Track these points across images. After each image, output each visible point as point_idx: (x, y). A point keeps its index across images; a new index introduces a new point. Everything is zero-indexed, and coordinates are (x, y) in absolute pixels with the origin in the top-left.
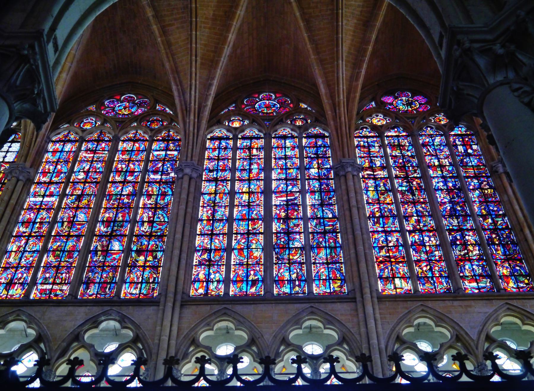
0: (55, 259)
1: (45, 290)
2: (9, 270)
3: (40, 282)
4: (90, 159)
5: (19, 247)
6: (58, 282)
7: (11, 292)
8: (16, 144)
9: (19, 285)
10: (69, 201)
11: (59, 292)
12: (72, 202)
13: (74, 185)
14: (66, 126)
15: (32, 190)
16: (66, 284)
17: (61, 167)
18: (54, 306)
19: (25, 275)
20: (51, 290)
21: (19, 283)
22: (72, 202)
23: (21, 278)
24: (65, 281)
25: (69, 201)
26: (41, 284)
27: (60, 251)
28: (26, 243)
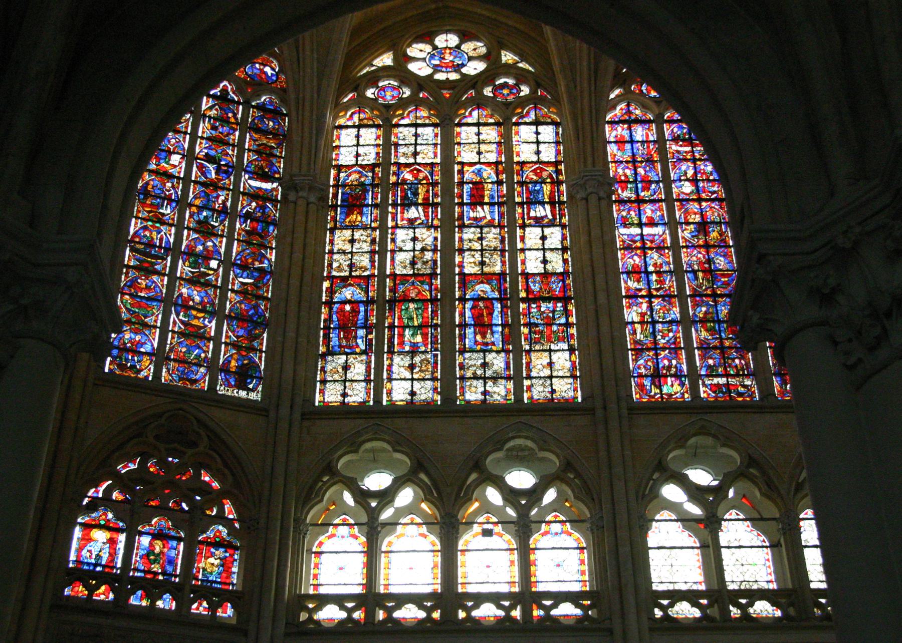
0: (711, 335)
1: (718, 385)
2: (644, 354)
3: (703, 372)
4: (689, 157)
5: (643, 315)
6: (732, 372)
7: (665, 390)
8: (545, 127)
9: (673, 379)
10: (687, 234)
11: (741, 389)
12: (693, 236)
13: (681, 204)
14: (617, 92)
15: (615, 215)
16: (748, 376)
17: (645, 171)
18: (754, 413)
19: (674, 362)
20: (727, 385)
21: (671, 376)
22: (693, 236)
23: (670, 367)
24: (744, 372)
25: (687, 234)
26: (707, 376)
27: (713, 322)
28: (651, 308)
